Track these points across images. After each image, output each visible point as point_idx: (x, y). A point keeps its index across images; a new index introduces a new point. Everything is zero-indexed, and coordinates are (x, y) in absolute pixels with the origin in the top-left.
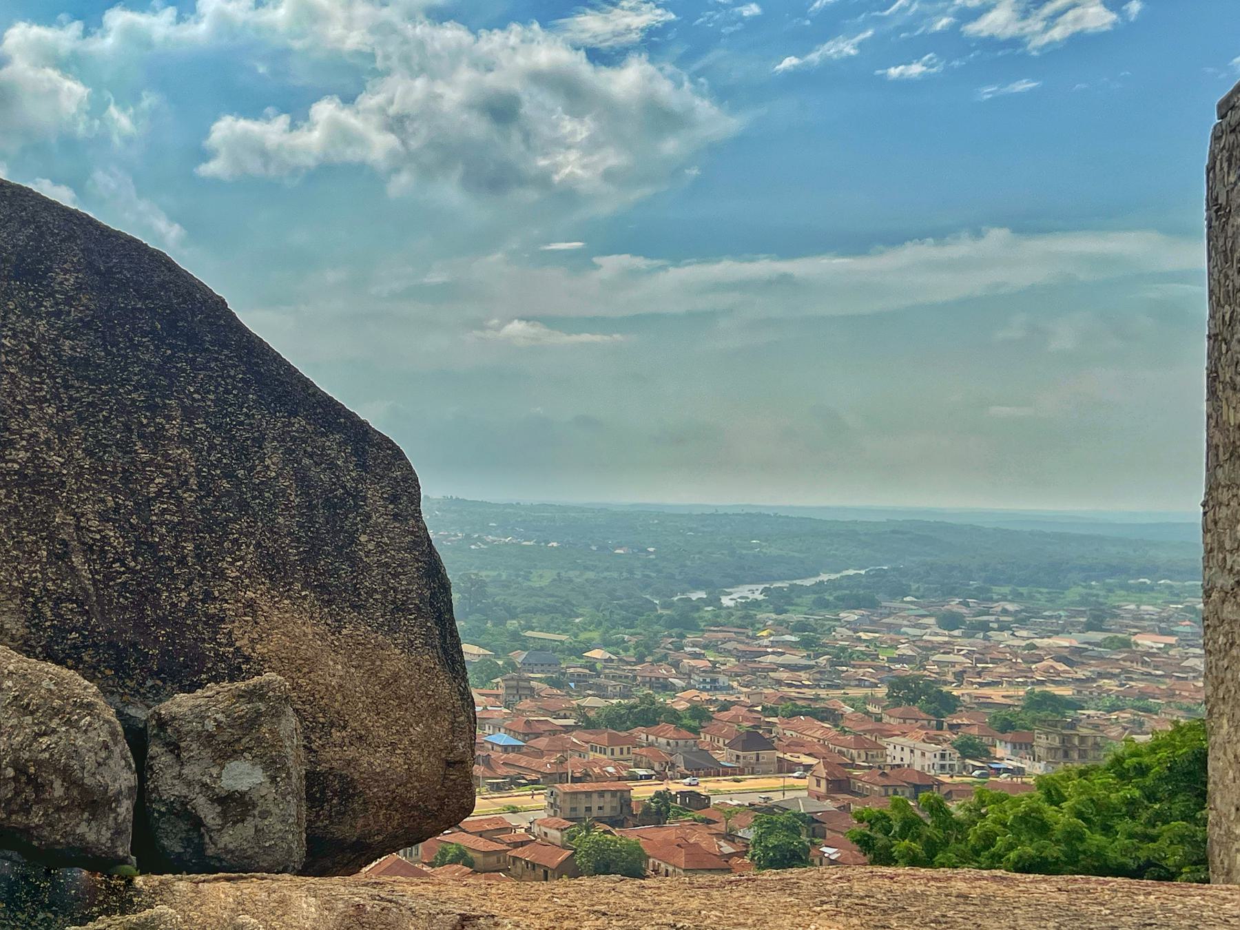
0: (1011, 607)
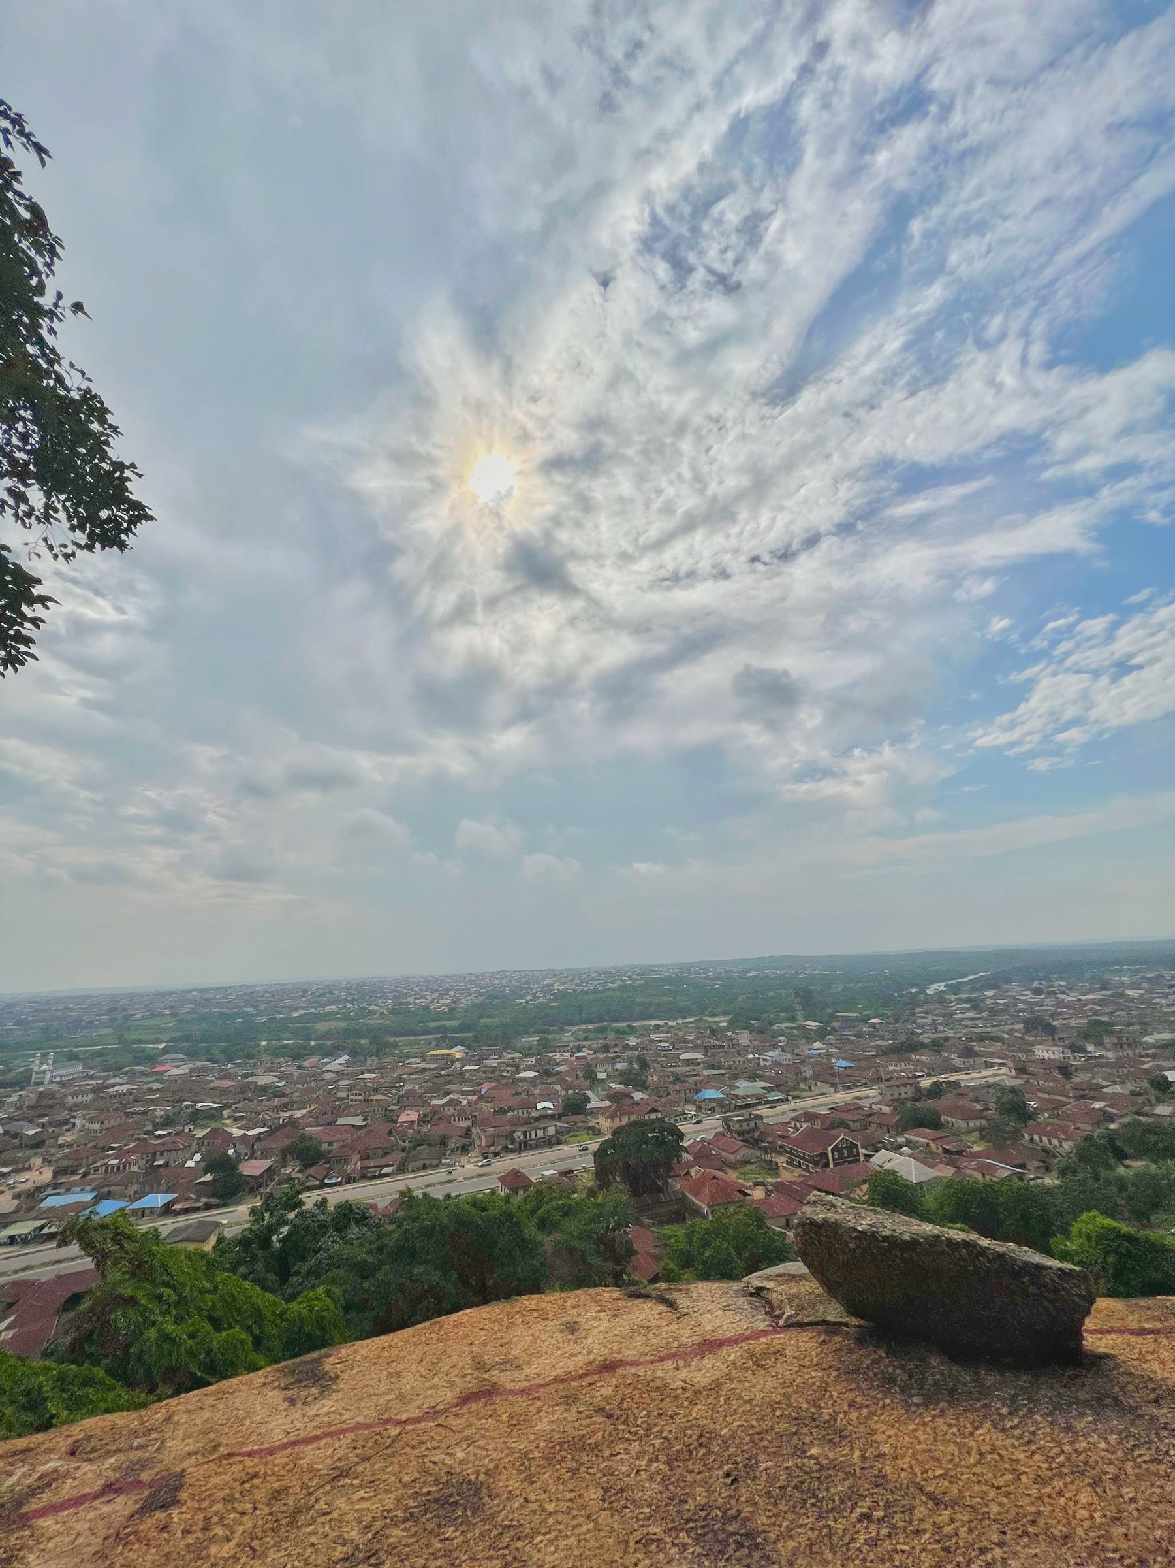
0: (1062, 983)
